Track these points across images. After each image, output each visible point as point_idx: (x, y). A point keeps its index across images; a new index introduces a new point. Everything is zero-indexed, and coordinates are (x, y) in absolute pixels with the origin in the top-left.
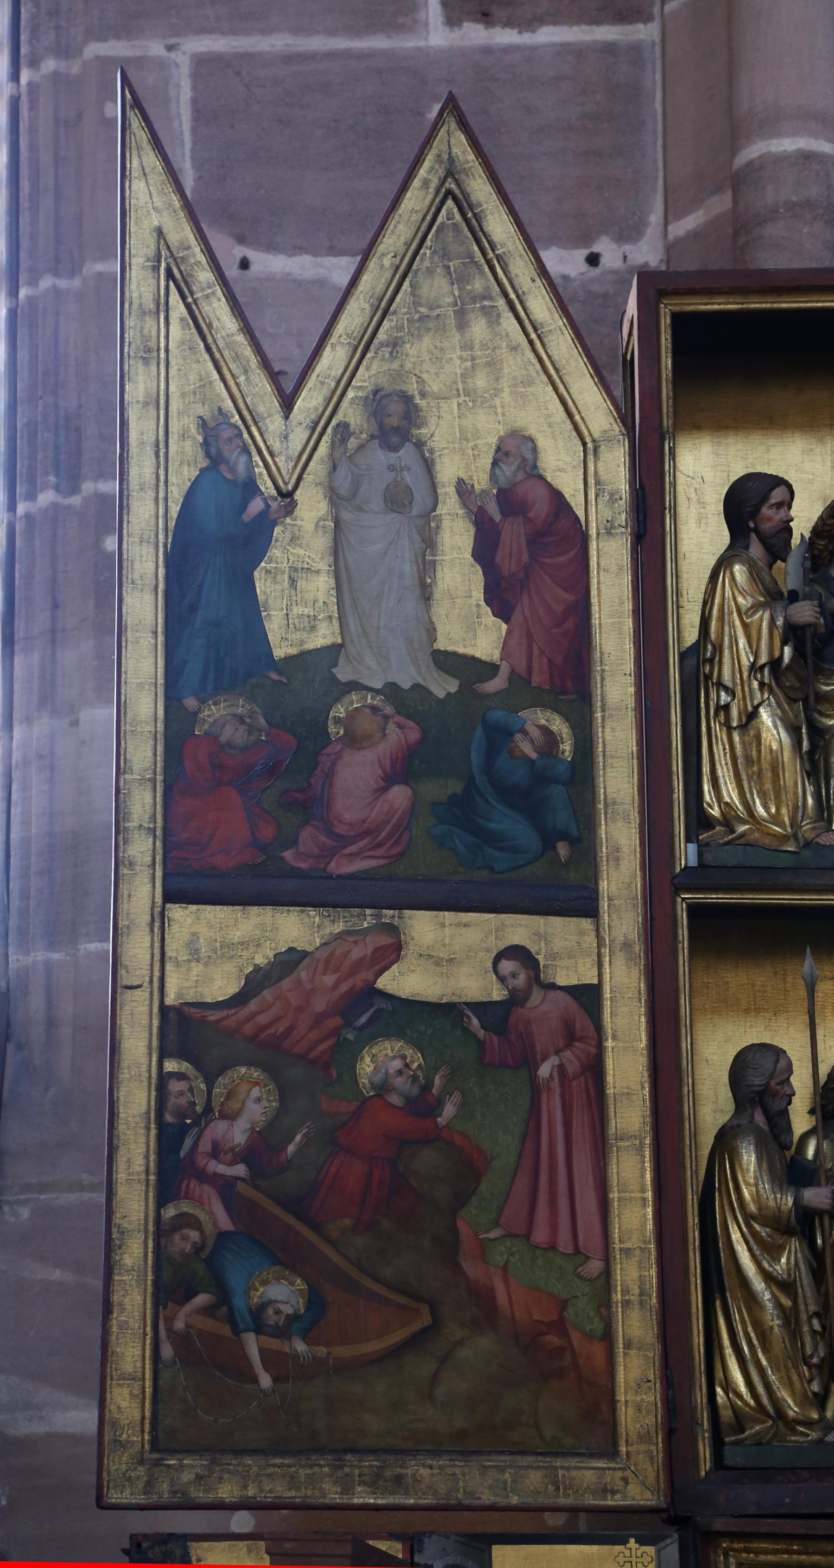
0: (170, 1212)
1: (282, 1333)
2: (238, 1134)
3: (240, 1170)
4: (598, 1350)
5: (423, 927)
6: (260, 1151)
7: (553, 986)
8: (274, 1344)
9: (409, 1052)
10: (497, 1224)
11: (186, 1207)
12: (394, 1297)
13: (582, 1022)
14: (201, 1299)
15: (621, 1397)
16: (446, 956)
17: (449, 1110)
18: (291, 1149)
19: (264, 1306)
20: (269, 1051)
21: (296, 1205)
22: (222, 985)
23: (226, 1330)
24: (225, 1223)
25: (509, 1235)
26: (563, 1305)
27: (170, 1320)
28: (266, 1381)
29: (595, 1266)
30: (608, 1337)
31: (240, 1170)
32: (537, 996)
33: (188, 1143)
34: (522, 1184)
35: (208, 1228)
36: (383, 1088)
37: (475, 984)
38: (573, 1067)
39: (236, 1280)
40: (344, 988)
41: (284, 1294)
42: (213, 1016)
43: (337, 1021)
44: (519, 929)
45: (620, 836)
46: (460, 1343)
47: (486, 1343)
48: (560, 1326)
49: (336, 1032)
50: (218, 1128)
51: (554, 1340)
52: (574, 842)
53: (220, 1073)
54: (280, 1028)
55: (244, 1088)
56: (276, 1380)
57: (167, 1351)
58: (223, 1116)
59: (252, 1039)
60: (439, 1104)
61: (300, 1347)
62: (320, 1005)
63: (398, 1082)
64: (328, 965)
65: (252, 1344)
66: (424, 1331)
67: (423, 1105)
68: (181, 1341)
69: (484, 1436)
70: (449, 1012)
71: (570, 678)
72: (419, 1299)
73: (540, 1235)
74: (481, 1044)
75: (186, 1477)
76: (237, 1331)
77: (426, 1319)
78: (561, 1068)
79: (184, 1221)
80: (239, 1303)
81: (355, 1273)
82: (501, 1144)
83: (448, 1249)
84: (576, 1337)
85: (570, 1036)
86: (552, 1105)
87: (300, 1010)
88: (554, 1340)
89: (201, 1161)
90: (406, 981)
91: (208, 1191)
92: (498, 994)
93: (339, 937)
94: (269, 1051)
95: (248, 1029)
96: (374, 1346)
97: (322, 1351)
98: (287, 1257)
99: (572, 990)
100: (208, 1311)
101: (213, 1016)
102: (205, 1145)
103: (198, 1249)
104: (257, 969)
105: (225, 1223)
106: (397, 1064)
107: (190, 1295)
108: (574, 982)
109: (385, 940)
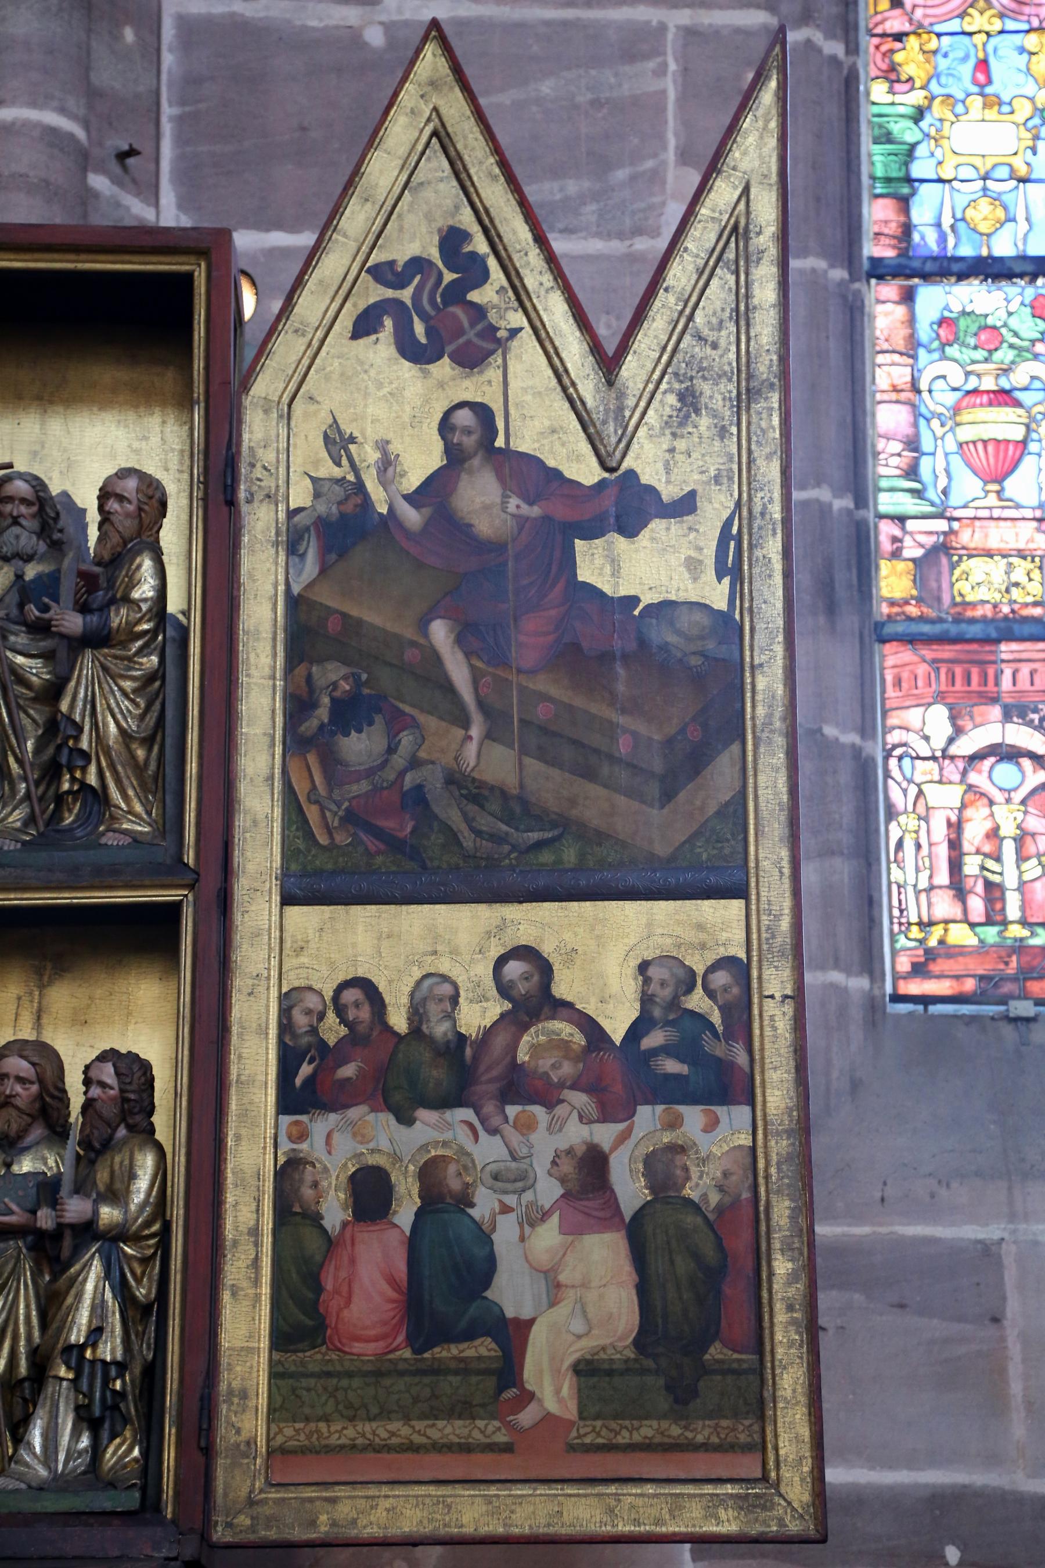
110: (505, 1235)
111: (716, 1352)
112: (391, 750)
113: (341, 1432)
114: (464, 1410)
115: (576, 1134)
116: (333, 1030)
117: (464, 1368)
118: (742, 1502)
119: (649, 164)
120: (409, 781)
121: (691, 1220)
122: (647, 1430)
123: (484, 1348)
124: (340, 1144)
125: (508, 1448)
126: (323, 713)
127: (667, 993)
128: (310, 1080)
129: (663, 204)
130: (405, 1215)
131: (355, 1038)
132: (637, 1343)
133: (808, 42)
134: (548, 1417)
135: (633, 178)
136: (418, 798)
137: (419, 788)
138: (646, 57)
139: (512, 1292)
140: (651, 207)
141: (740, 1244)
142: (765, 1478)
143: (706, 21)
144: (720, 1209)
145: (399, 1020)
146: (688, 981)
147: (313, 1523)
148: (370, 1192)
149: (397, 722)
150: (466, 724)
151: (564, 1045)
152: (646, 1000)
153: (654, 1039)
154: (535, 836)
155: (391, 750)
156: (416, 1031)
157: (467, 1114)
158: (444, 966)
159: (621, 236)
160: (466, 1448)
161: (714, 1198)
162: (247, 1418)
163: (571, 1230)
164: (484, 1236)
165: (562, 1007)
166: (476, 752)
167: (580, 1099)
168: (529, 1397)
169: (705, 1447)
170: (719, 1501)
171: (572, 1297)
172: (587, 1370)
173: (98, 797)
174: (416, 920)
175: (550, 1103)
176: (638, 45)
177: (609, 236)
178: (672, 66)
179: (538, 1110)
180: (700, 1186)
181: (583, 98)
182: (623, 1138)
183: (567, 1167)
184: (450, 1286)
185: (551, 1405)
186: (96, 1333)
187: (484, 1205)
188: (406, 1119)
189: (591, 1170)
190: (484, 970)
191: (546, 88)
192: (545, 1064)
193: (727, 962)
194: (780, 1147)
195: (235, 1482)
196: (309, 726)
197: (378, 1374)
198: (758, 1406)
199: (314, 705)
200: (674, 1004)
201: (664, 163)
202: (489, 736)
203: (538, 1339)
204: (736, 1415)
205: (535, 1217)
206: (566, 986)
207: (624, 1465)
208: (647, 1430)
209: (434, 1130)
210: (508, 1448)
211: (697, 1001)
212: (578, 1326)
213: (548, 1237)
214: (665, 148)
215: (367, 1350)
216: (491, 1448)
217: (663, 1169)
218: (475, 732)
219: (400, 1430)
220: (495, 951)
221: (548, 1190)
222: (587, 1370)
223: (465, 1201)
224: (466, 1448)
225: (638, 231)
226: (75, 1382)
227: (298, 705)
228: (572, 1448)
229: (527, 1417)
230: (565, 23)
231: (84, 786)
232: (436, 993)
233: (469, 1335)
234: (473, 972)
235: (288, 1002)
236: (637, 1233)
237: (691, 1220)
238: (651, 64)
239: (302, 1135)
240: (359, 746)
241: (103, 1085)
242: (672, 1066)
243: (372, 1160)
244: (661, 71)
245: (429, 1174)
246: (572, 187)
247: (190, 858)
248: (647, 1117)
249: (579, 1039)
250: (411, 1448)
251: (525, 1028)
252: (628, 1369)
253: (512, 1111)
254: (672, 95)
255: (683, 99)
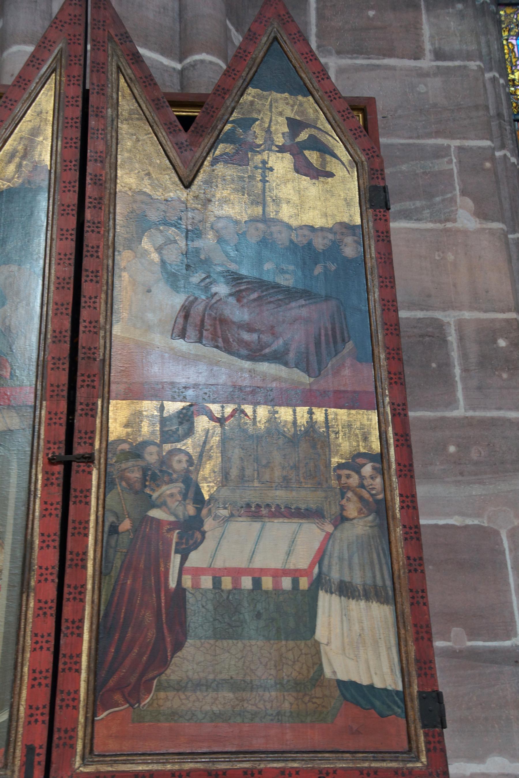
119: (449, 195)
129: (457, 210)
133: (505, 155)
135: (443, 200)
138: (443, 157)
140: (452, 211)
143: (467, 144)
159: (440, 222)
176: (440, 153)
177: (435, 222)
178: (454, 160)
181: (419, 171)
191: (404, 167)
201: (455, 195)
214: (455, 190)
225: (447, 220)
230: (409, 145)
238: (446, 160)
244: (450, 162)
246: (418, 204)
254: (455, 171)
255: (460, 172)
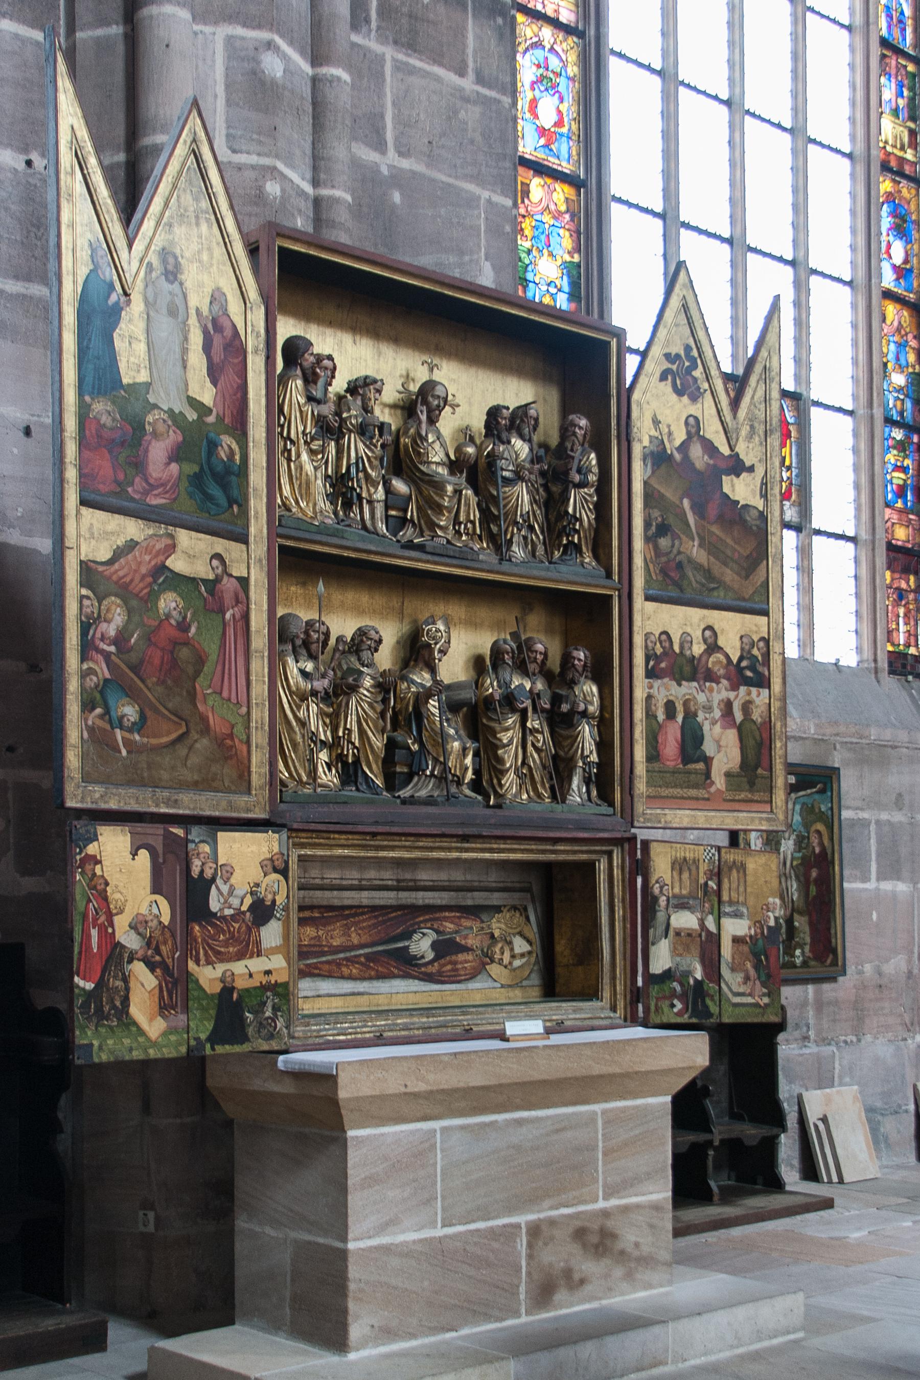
0: (85, 666)
1: (130, 730)
2: (111, 630)
3: (112, 649)
4: (245, 748)
5: (184, 537)
6: (120, 640)
7: (231, 575)
8: (127, 735)
9: (178, 599)
10: (210, 687)
11: (92, 665)
12: (173, 717)
13: (242, 595)
14: (99, 711)
15: (253, 769)
16: (192, 554)
17: (193, 630)
18: (133, 641)
19: (123, 716)
20: (124, 591)
21: (135, 669)
22: (104, 554)
23: (108, 727)
24: (108, 676)
25: (215, 692)
26: (233, 727)
27: (86, 720)
28: (124, 752)
29: (244, 710)
30: (248, 743)
31: (112, 649)
32: (225, 579)
33: (91, 632)
34: (219, 668)
35: (100, 676)
36: (168, 616)
37: (203, 570)
38: (238, 616)
39: (111, 702)
40: (153, 563)
41: (130, 712)
42: (101, 568)
43: (150, 579)
44: (220, 545)
45: (257, 506)
46: (196, 741)
47: (205, 741)
48: (231, 736)
49: (150, 584)
50: (103, 626)
51: (229, 742)
52: (240, 506)
53: (104, 598)
54: (128, 579)
55: (113, 607)
56: (128, 752)
57: (86, 735)
58: (105, 621)
59: (116, 583)
60: (190, 626)
61: (137, 737)
62: (143, 570)
63: (174, 613)
64: (148, 550)
65: (119, 734)
66: (184, 734)
67: (183, 627)
68: (91, 730)
69: (204, 784)
70: (192, 581)
71: (239, 424)
72: (181, 718)
73: (225, 694)
74: (205, 599)
75: (97, 795)
76: (113, 728)
77: (184, 729)
78: (234, 615)
79: (91, 672)
80: (113, 713)
81: (158, 704)
82: (211, 648)
83: (192, 696)
84: (236, 741)
85: (238, 601)
86: (230, 632)
87: (136, 571)
88: (229, 742)
89: (97, 642)
90: (177, 564)
91: (100, 658)
92: (211, 577)
93: (151, 536)
94: (124, 591)
95: (115, 578)
96: (165, 740)
97: (145, 740)
98: (132, 694)
99: (237, 578)
100: (101, 717)
101: (101, 568)
102: (98, 635)
103: (97, 686)
104: (118, 547)
105: (108, 676)
106: (173, 605)
107: (93, 709)
108: (239, 575)
109: (169, 542)
110: (706, 727)
111: (760, 771)
112: (673, 546)
113: (665, 792)
114: (696, 786)
115: (725, 694)
116: (659, 650)
117: (696, 772)
118: (768, 820)
120: (678, 558)
121: (754, 727)
122: (743, 796)
123: (701, 766)
124: (668, 690)
125: (708, 799)
126: (654, 528)
127: (747, 647)
128: (653, 667)
130: (680, 718)
131: (665, 653)
132: (741, 767)
134: (718, 790)
136: (680, 566)
137: (680, 562)
139: (708, 748)
141: (765, 736)
142: (772, 811)
144: (761, 724)
145: (677, 649)
146: (753, 645)
147: (660, 822)
148: (670, 708)
149: (675, 537)
150: (693, 540)
151: (721, 662)
152: (742, 649)
153: (744, 664)
154: (712, 585)
155: (673, 546)
156: (681, 652)
157: (695, 684)
158: (689, 630)
160: (697, 799)
161: (760, 720)
162: (641, 787)
163: (724, 728)
164: (701, 728)
165: (720, 649)
166: (695, 551)
167: (725, 682)
168: (713, 783)
169: (757, 801)
170: (761, 819)
171: (724, 750)
172: (728, 775)
173: (578, 548)
174: (681, 611)
175: (718, 683)
179: (714, 685)
180: (756, 716)
182: (737, 696)
183: (722, 706)
184: (692, 743)
185: (719, 786)
186: (591, 752)
187: (700, 717)
188: (680, 685)
189: (728, 706)
190: (699, 633)
192: (716, 669)
193: (762, 639)
194: (776, 705)
195: (639, 807)
196: (650, 533)
197: (674, 773)
198: (771, 789)
199: (651, 525)
200: (749, 652)
202: (700, 546)
203: (715, 762)
204: (764, 792)
205: (714, 723)
206: (721, 642)
207: (737, 806)
208: (743, 796)
209: (688, 689)
210: (708, 799)
211: (755, 652)
212: (725, 760)
213: (717, 728)
215: (670, 764)
216: (704, 799)
217: (746, 707)
218: (696, 543)
219: (678, 792)
220: (703, 627)
221: (717, 714)
222: (728, 775)
223: (695, 715)
224: (697, 799)
226: (584, 770)
227: (647, 524)
228: (725, 800)
229: (713, 789)
231: (573, 542)
232: (687, 640)
233: (697, 761)
234: (697, 634)
235: (647, 636)
236: (740, 729)
237: (754, 727)
239: (651, 687)
240: (664, 542)
241: (579, 660)
242: (749, 674)
243: (671, 698)
245: (686, 703)
247: (616, 577)
248: (743, 689)
249: (725, 661)
250: (683, 798)
251: (710, 655)
252: (738, 776)
253: (708, 684)
